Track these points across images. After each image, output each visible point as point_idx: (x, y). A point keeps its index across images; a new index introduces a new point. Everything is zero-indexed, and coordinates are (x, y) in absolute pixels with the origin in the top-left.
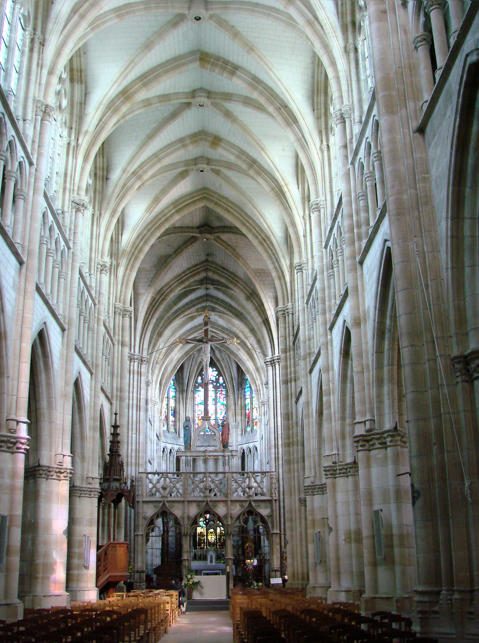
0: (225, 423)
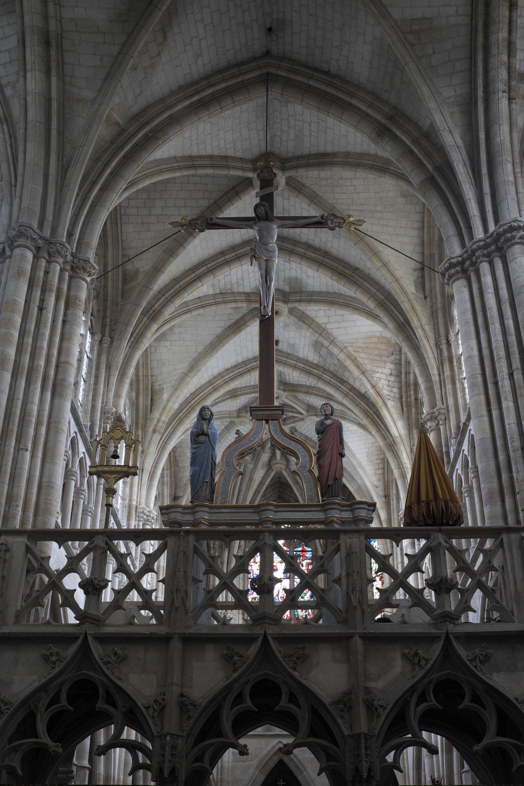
0: (329, 422)
